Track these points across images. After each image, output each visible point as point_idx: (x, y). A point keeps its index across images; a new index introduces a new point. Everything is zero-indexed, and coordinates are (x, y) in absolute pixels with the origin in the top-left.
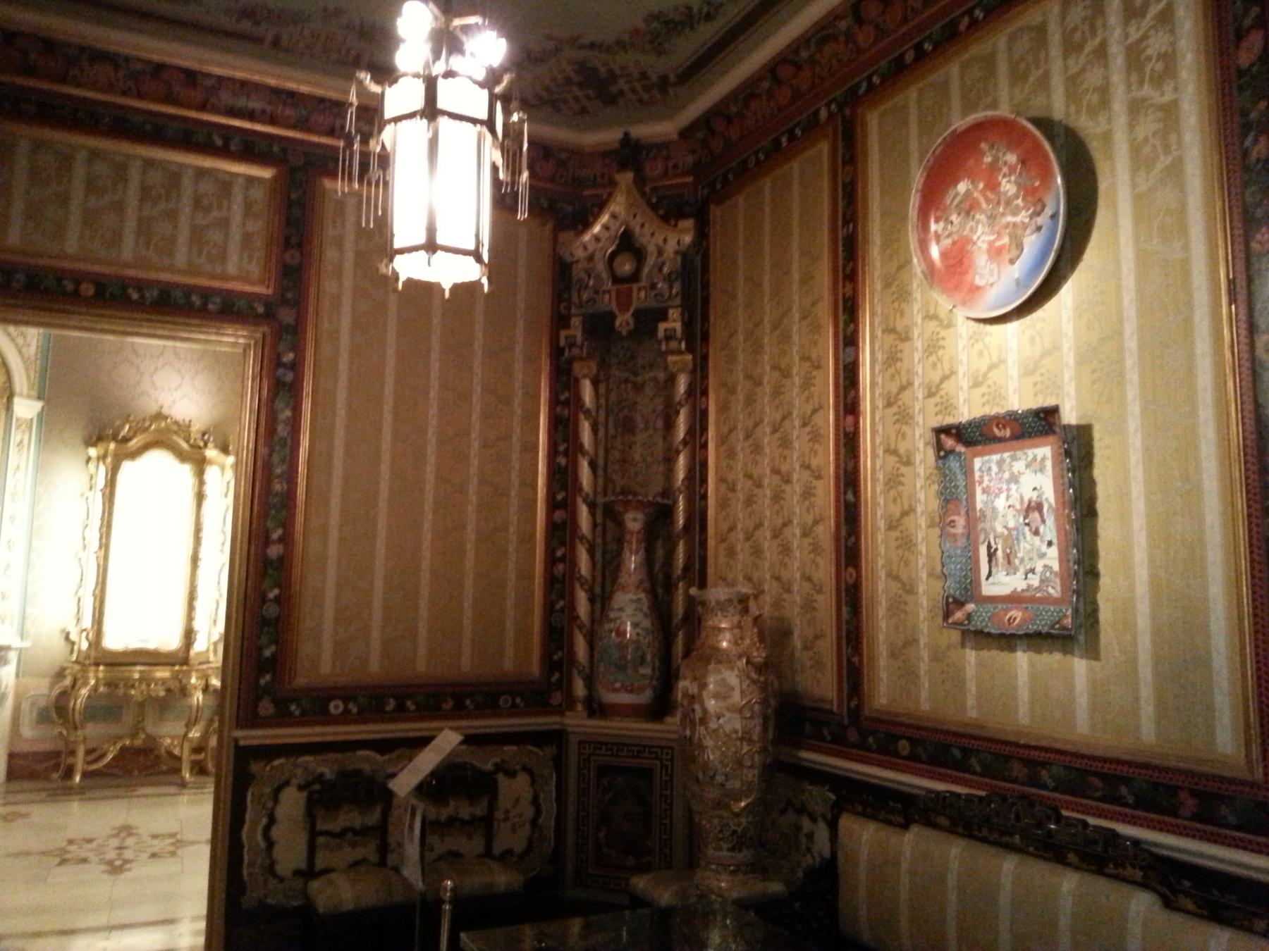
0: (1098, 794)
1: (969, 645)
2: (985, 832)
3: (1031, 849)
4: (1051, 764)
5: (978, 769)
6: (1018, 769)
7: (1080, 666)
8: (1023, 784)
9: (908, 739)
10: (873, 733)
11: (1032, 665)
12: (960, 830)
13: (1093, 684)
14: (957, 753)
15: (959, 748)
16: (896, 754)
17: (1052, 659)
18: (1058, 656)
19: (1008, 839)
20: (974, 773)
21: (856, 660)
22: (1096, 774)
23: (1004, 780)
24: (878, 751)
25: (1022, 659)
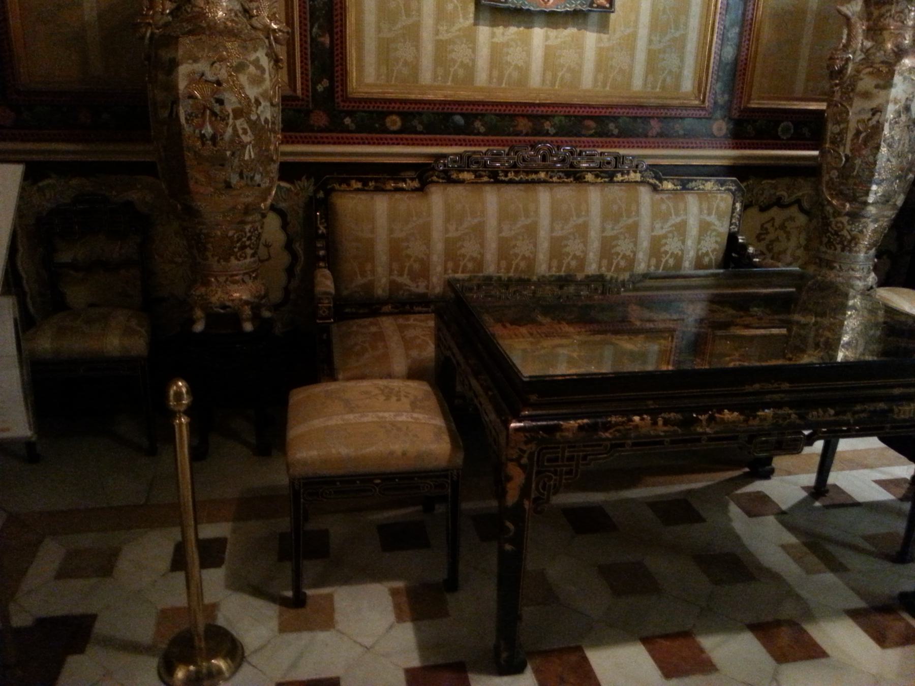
0: (592, 132)
1: (481, 22)
2: (511, 175)
3: (555, 179)
4: (553, 116)
5: (482, 129)
6: (523, 124)
7: (591, 38)
8: (527, 135)
9: (399, 114)
10: (350, 114)
11: (547, 38)
12: (485, 179)
13: (600, 51)
14: (459, 120)
15: (462, 115)
16: (386, 131)
17: (569, 32)
18: (571, 31)
19: (534, 176)
20: (479, 134)
21: (326, 40)
22: (591, 118)
23: (509, 135)
24: (359, 130)
25: (539, 34)
